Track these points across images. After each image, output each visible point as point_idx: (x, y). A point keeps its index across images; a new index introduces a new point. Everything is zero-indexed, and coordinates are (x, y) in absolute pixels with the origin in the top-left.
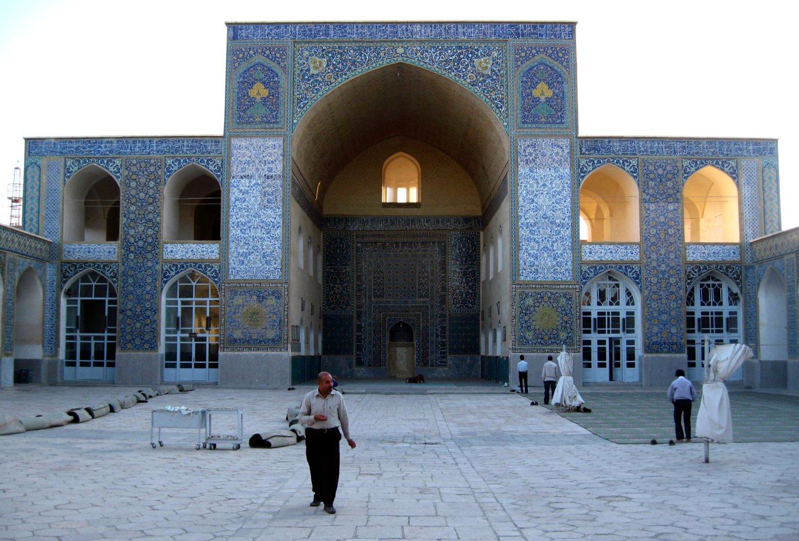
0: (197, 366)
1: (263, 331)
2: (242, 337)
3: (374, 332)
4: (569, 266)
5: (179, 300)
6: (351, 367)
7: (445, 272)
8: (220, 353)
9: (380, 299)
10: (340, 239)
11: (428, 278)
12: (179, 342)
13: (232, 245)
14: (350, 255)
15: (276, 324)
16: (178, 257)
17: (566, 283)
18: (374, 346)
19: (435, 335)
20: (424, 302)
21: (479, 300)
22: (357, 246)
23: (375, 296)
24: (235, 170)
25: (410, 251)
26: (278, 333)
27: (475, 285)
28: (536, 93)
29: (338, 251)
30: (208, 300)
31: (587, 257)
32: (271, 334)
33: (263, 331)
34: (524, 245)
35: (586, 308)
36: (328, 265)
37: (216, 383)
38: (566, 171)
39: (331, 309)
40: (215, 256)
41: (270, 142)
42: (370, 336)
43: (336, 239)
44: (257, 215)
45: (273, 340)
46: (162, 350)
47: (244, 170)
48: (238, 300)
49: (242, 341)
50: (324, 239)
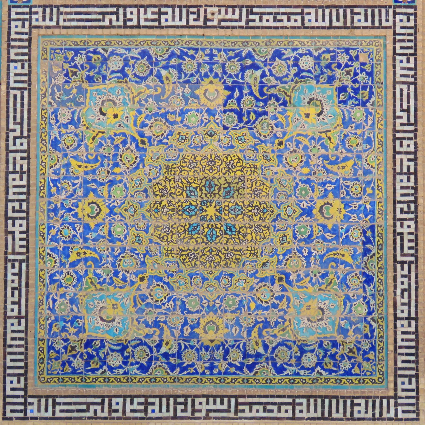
1: (265, 294)
2: (136, 332)
15: (346, 253)
26: (361, 310)
33: (265, 294)
49: (141, 355)
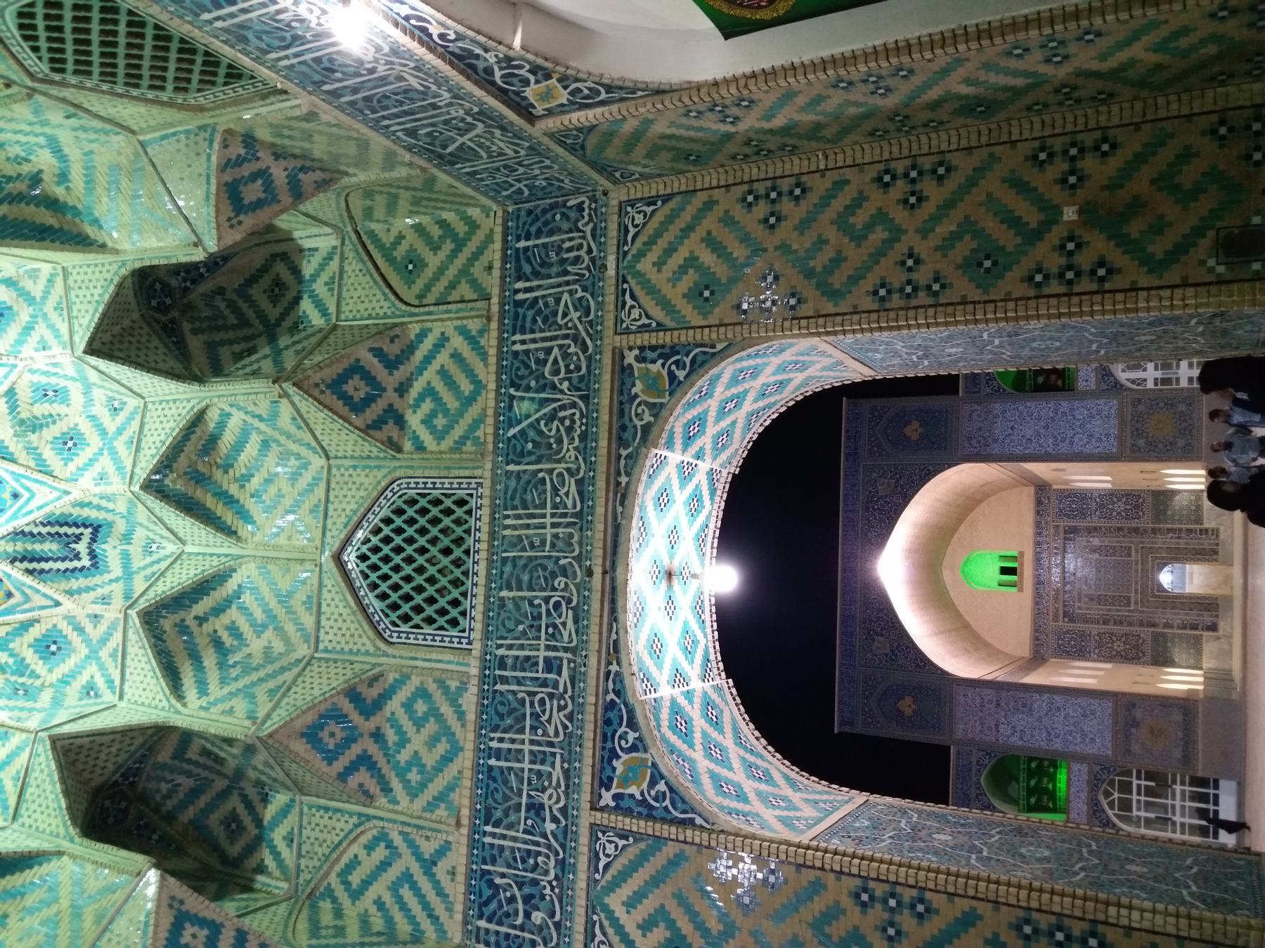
0: (1216, 803)
4: (1101, 402)
5: (1135, 813)
6: (1218, 638)
8: (1200, 774)
12: (1187, 820)
13: (1072, 748)
16: (1085, 808)
17: (1120, 409)
23: (1128, 605)
24: (990, 738)
28: (915, 436)
30: (1135, 782)
31: (1092, 385)
32: (1178, 717)
34: (1077, 449)
35: (1150, 385)
37: (1239, 784)
38: (997, 407)
40: (1084, 768)
41: (962, 700)
44: (1040, 719)
45: (1185, 715)
46: (1197, 839)
47: (990, 729)
48: (1136, 748)
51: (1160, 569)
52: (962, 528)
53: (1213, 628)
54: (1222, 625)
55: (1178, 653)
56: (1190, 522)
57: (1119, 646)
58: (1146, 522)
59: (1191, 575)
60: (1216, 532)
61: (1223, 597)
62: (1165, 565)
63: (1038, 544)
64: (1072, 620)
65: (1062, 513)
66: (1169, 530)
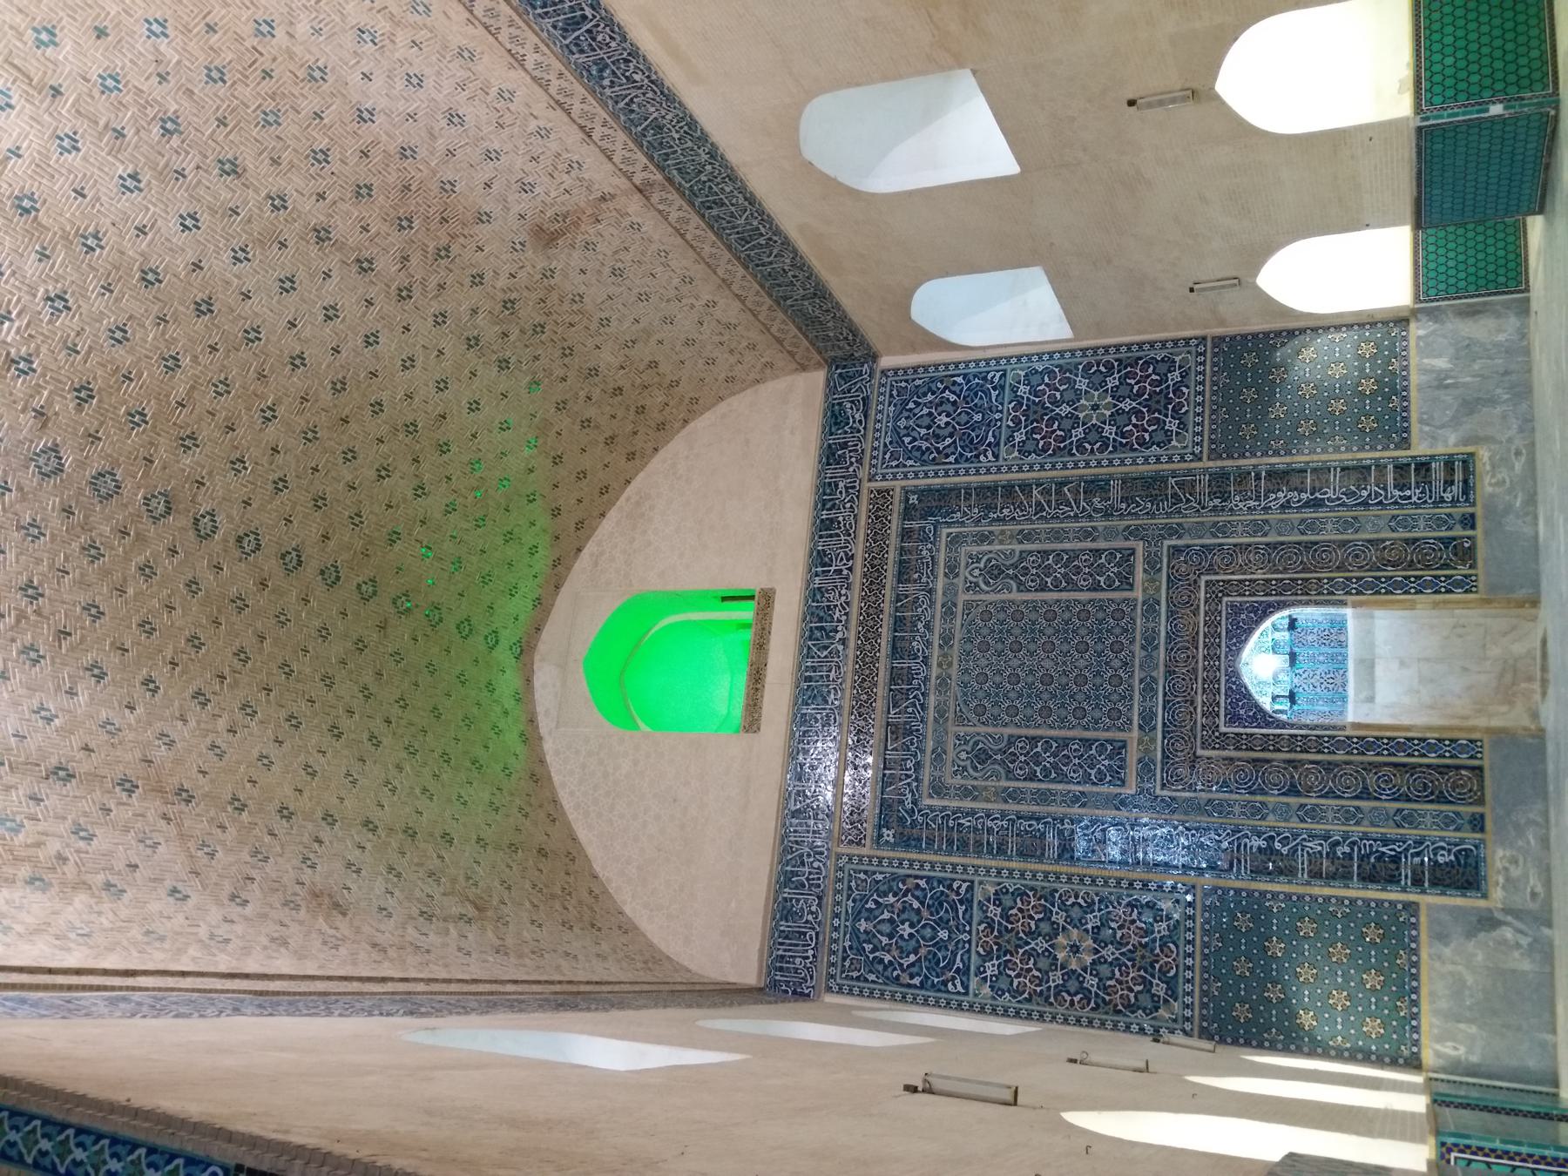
3: (1293, 791)
6: (1488, 922)
7: (1026, 487)
9: (1133, 755)
10: (857, 918)
11: (1046, 553)
14: (929, 879)
18: (1365, 794)
19: (1308, 514)
20: (1152, 564)
21: (1152, 344)
22: (893, 846)
25: (928, 626)
27: (1089, 365)
29: (906, 930)
36: (966, 987)
39: (1172, 993)
42: (1313, 813)
43: (855, 931)
50: (850, 993)
51: (1240, 634)
52: (607, 526)
53: (1463, 874)
54: (1498, 858)
55: (1321, 991)
56: (1363, 438)
57: (1073, 949)
58: (1187, 453)
59: (1367, 665)
60: (1461, 469)
61: (1502, 737)
62: (1264, 612)
63: (819, 559)
64: (906, 841)
65: (901, 448)
66: (1279, 477)
